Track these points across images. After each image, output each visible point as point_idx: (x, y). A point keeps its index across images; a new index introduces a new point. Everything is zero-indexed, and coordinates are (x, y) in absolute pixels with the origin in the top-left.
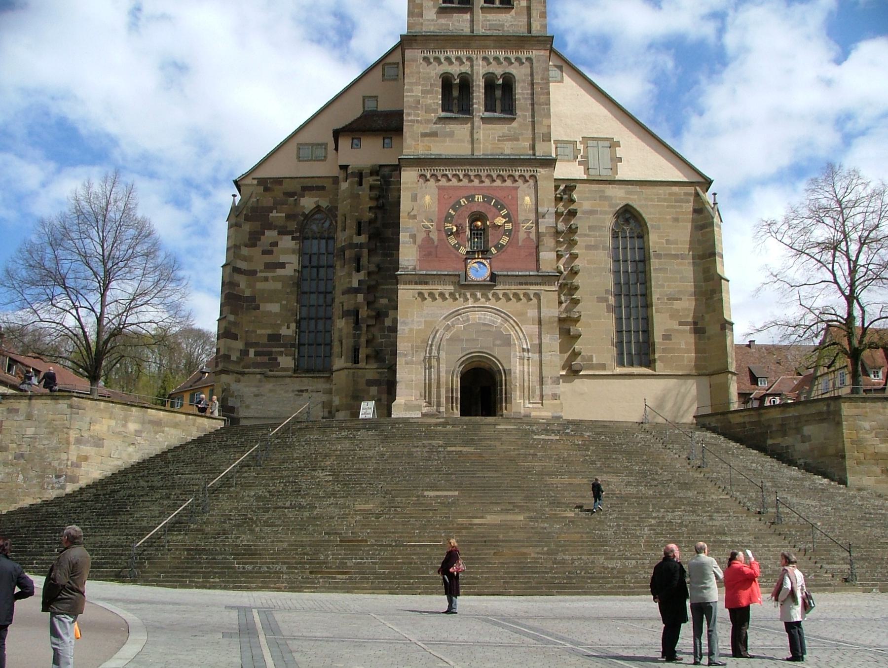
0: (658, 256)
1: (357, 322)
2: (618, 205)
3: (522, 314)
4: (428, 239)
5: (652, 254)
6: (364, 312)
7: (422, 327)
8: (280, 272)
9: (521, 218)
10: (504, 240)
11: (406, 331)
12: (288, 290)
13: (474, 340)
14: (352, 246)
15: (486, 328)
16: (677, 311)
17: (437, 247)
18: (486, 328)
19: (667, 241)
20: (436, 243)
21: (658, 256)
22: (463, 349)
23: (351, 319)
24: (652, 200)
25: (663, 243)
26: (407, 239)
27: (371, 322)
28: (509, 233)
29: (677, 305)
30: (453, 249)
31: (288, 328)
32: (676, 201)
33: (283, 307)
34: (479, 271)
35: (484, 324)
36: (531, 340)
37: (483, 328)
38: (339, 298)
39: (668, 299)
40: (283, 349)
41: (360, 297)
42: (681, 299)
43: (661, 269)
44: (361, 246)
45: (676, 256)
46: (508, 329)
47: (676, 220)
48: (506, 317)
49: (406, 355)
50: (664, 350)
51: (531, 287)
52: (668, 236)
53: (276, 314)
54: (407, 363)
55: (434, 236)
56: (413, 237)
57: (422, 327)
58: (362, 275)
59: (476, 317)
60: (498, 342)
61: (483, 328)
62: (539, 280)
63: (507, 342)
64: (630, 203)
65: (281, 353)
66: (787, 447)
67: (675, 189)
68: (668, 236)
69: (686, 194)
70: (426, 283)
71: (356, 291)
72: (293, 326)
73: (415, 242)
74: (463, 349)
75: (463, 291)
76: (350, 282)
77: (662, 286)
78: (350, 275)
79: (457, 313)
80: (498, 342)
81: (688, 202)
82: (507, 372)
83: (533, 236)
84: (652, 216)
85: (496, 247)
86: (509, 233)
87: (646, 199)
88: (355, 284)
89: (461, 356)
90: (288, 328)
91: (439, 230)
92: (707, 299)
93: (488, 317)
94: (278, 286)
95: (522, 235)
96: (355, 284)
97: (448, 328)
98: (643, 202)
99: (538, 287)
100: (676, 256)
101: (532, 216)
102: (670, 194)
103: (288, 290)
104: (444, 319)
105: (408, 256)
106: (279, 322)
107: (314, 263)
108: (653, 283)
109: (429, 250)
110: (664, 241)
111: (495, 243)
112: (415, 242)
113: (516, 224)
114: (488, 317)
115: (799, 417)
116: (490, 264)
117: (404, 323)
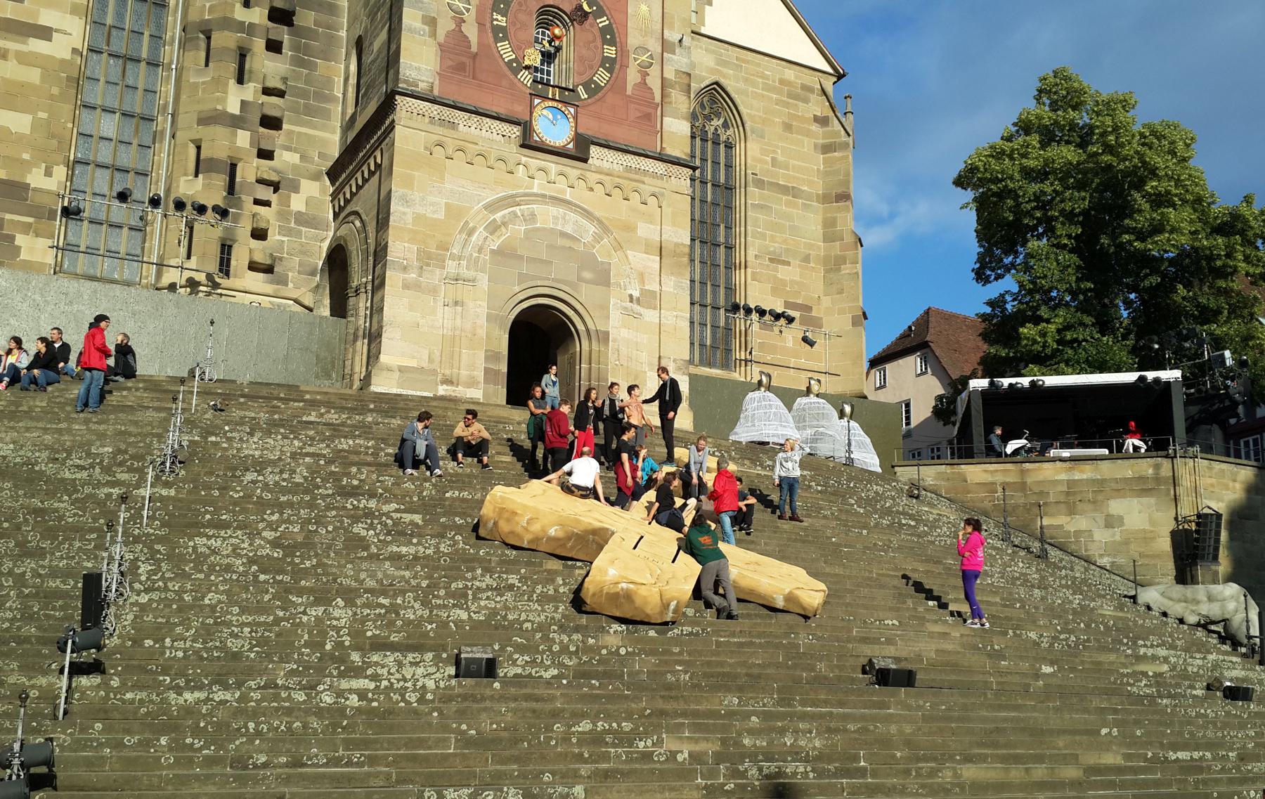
0: (760, 184)
1: (231, 188)
2: (703, 79)
3: (630, 228)
4: (458, 36)
5: (750, 177)
6: (250, 169)
7: (441, 215)
8: (37, 46)
9: (633, 40)
10: (602, 77)
11: (409, 218)
12: (55, 91)
13: (542, 261)
14: (228, 23)
15: (567, 243)
16: (784, 283)
17: (475, 56)
18: (567, 243)
19: (773, 159)
20: (474, 49)
21: (760, 184)
22: (522, 277)
23: (221, 181)
24: (754, 84)
25: (766, 163)
26: (418, 24)
27: (265, 193)
28: (609, 64)
29: (783, 273)
30: (505, 69)
31: (48, 173)
32: (790, 96)
33: (34, 126)
34: (554, 128)
35: (564, 235)
36: (642, 281)
37: (561, 242)
38: (189, 130)
39: (771, 260)
40: (31, 220)
41: (243, 139)
42: (788, 264)
43: (761, 207)
44: (250, 29)
45: (785, 190)
46: (602, 251)
47: (788, 127)
48: (606, 229)
49: (405, 269)
50: (762, 345)
51: (646, 179)
52: (774, 152)
53: (20, 138)
54: (406, 286)
55: (471, 31)
56: (431, 22)
57: (441, 215)
58: (250, 91)
59: (548, 216)
60: (587, 275)
61: (561, 242)
62: (660, 167)
63: (603, 278)
64: (723, 81)
65: (26, 229)
66: (1078, 533)
67: (790, 73)
68: (774, 152)
69: (807, 88)
70: (453, 126)
71: (236, 122)
72: (60, 172)
73: (433, 34)
74: (522, 277)
75: (524, 159)
76: (223, 100)
77: (763, 236)
78: (219, 83)
79: (511, 201)
80: (587, 275)
81: (806, 101)
82: (604, 337)
83: (654, 82)
84: (753, 113)
85: (586, 86)
86: (609, 64)
87: (746, 80)
88: (234, 108)
89: (517, 289)
90: (48, 173)
91: (481, 25)
92: (826, 271)
93: (571, 222)
94: (33, 75)
95: (633, 76)
96: (234, 108)
97: (493, 228)
98: (741, 85)
99: (659, 183)
100: (785, 190)
101: (655, 47)
102: (782, 82)
103: (55, 91)
104: (486, 207)
105: (419, 62)
106: (26, 156)
107: (119, 45)
108: (749, 228)
109: (459, 57)
110: (769, 159)
111: (585, 78)
112: (433, 34)
113: (623, 51)
114: (571, 222)
115: (1102, 482)
116: (576, 118)
117: (405, 200)
